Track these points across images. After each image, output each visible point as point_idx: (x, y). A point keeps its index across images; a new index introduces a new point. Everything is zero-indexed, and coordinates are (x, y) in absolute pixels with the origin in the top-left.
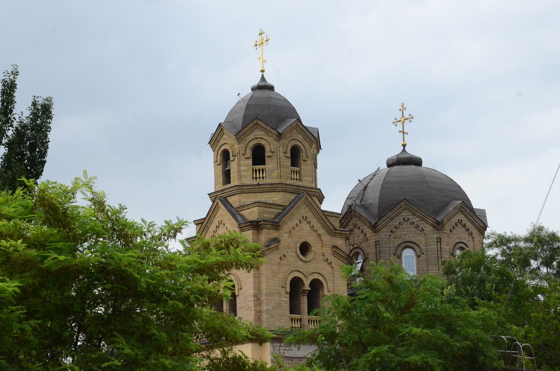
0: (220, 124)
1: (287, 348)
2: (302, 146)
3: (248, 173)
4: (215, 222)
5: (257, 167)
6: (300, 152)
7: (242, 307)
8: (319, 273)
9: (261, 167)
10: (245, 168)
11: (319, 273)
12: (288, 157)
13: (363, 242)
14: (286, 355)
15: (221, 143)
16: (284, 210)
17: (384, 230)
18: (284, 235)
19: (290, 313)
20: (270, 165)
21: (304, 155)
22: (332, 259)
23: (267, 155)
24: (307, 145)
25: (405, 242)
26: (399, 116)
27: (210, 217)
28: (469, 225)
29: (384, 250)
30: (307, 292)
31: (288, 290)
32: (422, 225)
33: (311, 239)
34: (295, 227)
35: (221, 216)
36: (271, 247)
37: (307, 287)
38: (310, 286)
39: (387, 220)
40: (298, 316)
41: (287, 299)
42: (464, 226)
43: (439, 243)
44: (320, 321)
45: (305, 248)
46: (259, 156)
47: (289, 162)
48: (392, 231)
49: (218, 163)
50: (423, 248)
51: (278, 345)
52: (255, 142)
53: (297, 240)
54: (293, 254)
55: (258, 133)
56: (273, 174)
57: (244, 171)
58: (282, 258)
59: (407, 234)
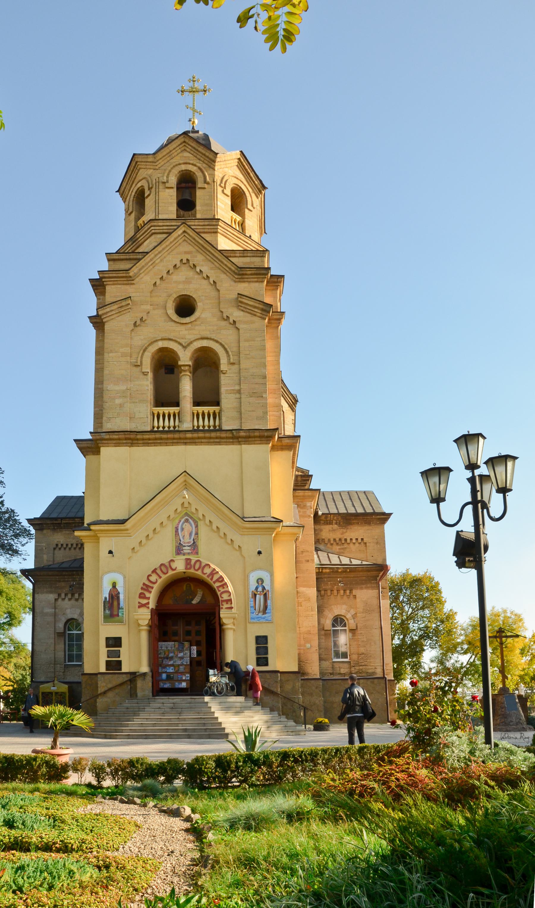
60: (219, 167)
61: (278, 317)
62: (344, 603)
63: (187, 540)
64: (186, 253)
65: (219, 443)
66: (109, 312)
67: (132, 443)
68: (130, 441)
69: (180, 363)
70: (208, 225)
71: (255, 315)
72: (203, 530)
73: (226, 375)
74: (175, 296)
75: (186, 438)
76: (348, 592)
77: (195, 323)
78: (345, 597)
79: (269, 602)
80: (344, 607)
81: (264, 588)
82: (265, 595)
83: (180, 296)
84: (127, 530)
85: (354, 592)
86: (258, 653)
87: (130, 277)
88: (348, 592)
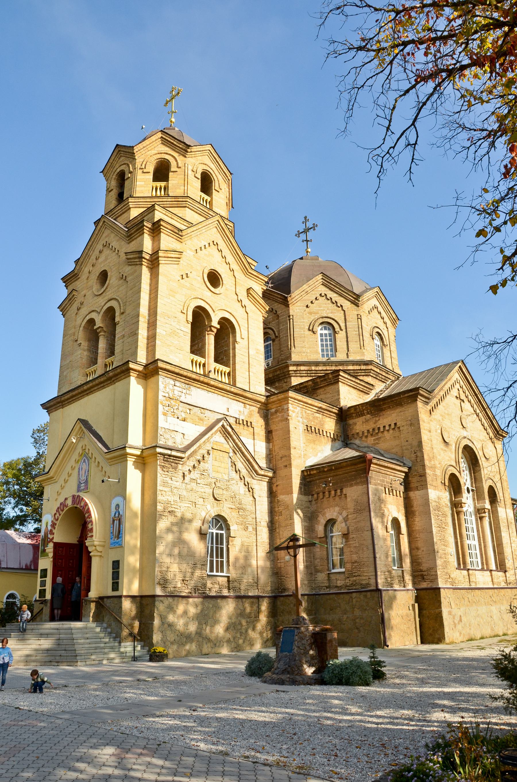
0: (117, 145)
1: (184, 391)
2: (214, 175)
3: (145, 189)
4: (100, 247)
5: (158, 184)
6: (211, 182)
7: (124, 336)
8: (230, 313)
9: (163, 184)
10: (143, 183)
11: (230, 313)
12: (199, 179)
13: (273, 320)
14: (183, 399)
15: (118, 165)
16: (189, 228)
17: (298, 304)
18: (188, 252)
19: (192, 352)
20: (174, 180)
21: (217, 184)
22: (246, 301)
23: (172, 169)
24: (220, 177)
25: (322, 318)
26: (302, 228)
27: (93, 242)
28: (383, 314)
29: (299, 325)
30: (215, 330)
31: (190, 319)
32: (341, 301)
33: (223, 271)
34: (203, 248)
35: (106, 237)
36: (169, 255)
37: (215, 323)
38: (219, 323)
39: (302, 294)
40: (203, 360)
41: (188, 329)
42: (380, 313)
43: (359, 320)
44: (229, 374)
45: (214, 279)
46: (162, 172)
47: (198, 184)
48: (307, 306)
49: (109, 190)
50: (343, 325)
51: (172, 382)
52: (159, 156)
53: (205, 265)
54: (200, 279)
55: (163, 149)
56: (178, 191)
57: (141, 186)
58: (184, 276)
59: (324, 310)
60: (139, 155)
61: (156, 257)
62: (337, 505)
63: (83, 478)
64: (106, 237)
65: (103, 387)
66: (65, 307)
67: (63, 405)
68: (61, 404)
69: (95, 327)
70: (124, 206)
71: (137, 265)
72: (93, 465)
73: (119, 325)
74: (98, 275)
75: (86, 391)
76: (339, 491)
77: (107, 290)
78: (337, 498)
79: (121, 526)
80: (337, 509)
81: (119, 513)
82: (119, 520)
83: (101, 273)
84: (52, 478)
85: (344, 492)
86: (113, 579)
87: (76, 274)
88: (339, 491)
